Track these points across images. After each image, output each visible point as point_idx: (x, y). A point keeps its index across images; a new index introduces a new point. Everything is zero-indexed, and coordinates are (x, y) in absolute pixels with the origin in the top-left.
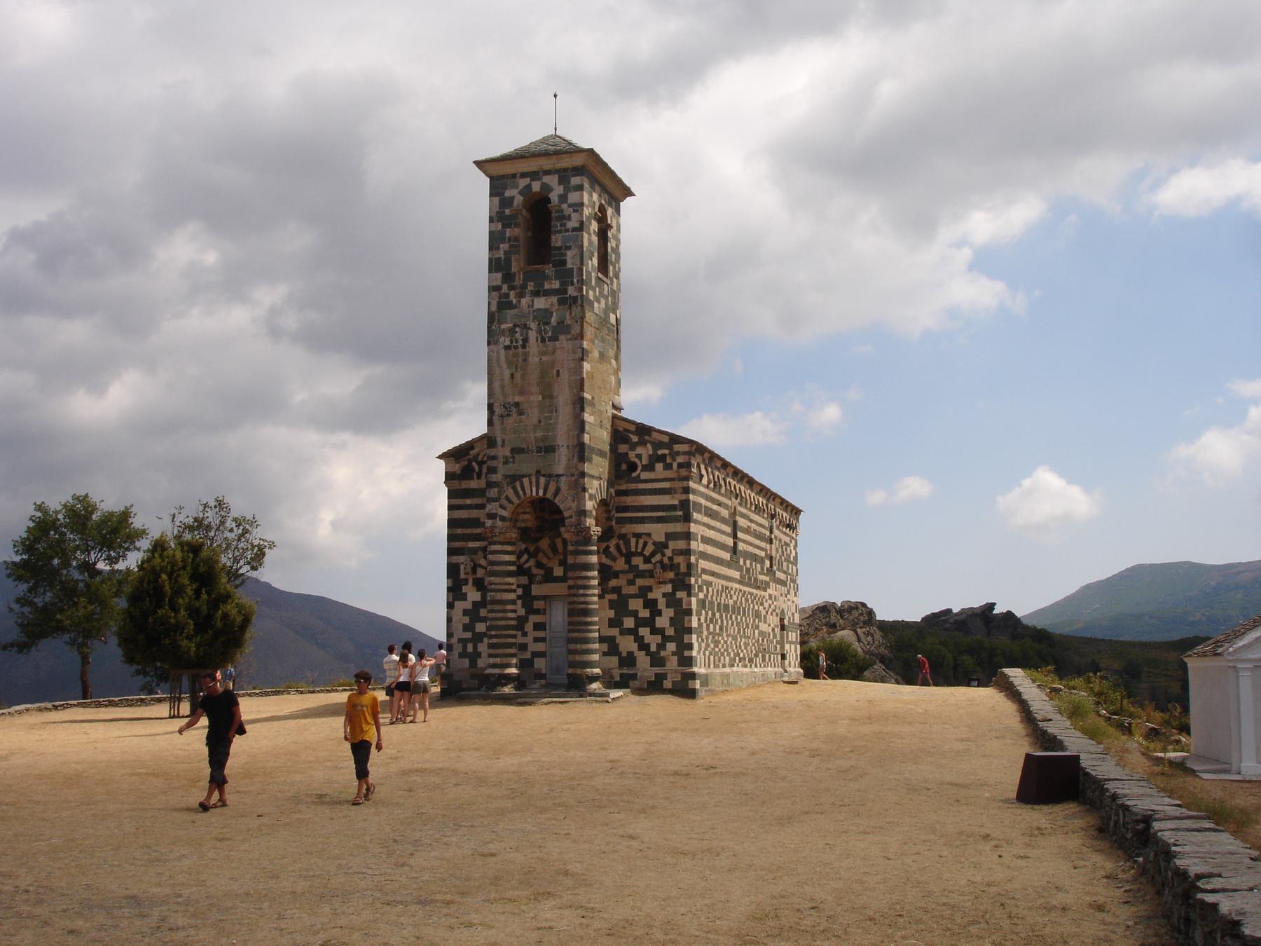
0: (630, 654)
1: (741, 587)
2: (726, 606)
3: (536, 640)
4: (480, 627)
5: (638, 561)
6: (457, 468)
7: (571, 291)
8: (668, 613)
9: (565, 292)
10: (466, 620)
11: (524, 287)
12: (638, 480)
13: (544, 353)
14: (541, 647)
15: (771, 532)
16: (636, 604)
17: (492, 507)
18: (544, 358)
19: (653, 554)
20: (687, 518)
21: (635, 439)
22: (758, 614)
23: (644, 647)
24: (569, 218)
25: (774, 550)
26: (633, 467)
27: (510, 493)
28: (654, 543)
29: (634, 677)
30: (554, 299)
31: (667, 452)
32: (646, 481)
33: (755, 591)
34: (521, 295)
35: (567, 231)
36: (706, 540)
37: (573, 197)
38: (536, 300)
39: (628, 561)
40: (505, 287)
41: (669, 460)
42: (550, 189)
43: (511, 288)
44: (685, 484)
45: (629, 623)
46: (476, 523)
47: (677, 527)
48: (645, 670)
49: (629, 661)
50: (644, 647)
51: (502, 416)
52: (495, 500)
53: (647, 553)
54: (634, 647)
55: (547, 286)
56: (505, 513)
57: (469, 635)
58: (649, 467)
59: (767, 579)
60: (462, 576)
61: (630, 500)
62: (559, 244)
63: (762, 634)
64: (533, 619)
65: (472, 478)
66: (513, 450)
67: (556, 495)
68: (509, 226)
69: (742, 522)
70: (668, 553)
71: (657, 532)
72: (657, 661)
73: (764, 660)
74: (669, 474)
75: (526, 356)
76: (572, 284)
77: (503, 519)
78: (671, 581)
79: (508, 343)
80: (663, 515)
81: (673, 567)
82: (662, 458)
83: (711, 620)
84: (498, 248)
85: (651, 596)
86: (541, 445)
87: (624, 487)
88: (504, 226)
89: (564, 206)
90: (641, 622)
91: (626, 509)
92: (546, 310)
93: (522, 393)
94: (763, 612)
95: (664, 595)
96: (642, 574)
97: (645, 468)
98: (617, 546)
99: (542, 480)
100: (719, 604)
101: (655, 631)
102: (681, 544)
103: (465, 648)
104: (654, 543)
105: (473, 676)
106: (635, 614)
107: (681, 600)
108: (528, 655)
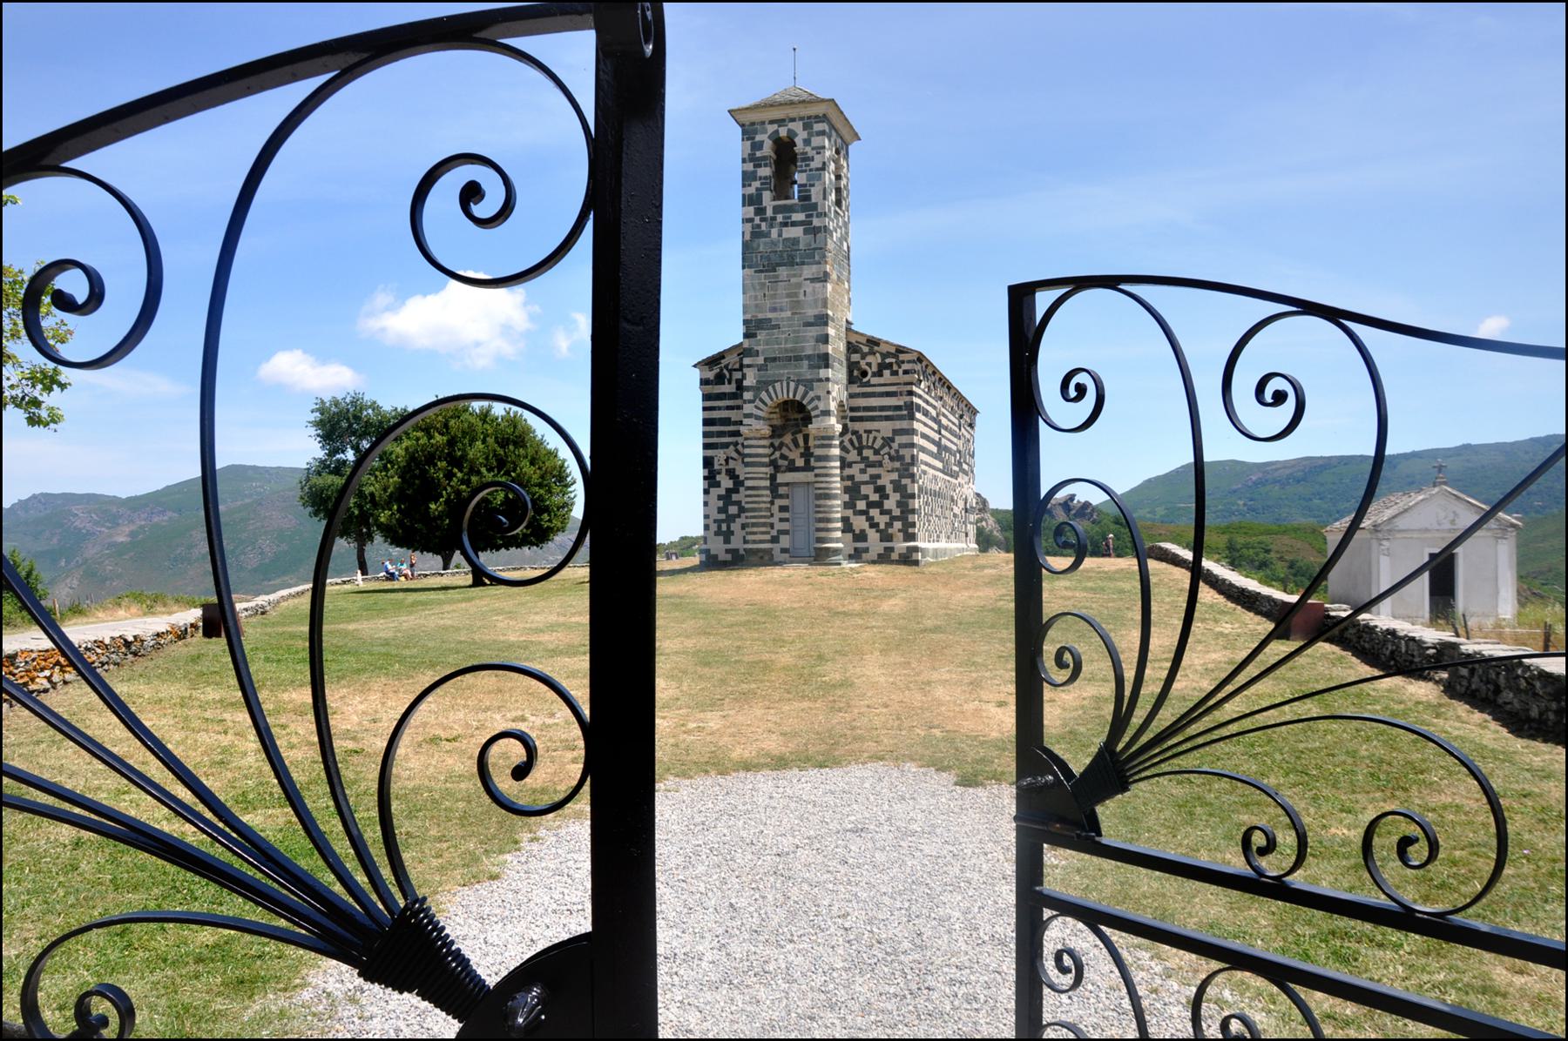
0: (863, 531)
3: (781, 520)
4: (733, 510)
5: (867, 453)
6: (711, 375)
7: (816, 222)
10: (721, 503)
11: (774, 219)
12: (868, 384)
14: (785, 526)
16: (867, 490)
17: (748, 408)
19: (883, 446)
20: (912, 417)
21: (866, 349)
23: (874, 525)
24: (812, 159)
25: (960, 443)
26: (864, 374)
27: (764, 395)
29: (866, 550)
34: (771, 226)
36: (924, 436)
37: (816, 141)
39: (860, 454)
41: (895, 367)
42: (796, 135)
43: (762, 220)
44: (908, 388)
45: (861, 505)
46: (726, 421)
47: (904, 424)
49: (861, 537)
50: (874, 525)
52: (750, 402)
53: (877, 446)
54: (866, 526)
56: (759, 413)
58: (879, 374)
60: (716, 467)
64: (779, 502)
69: (944, 421)
70: (895, 446)
71: (886, 428)
72: (886, 537)
74: (894, 379)
81: (900, 458)
85: (880, 482)
89: (808, 149)
90: (871, 505)
96: (872, 465)
97: (874, 375)
98: (851, 441)
99: (792, 385)
103: (719, 527)
106: (866, 497)
108: (774, 533)
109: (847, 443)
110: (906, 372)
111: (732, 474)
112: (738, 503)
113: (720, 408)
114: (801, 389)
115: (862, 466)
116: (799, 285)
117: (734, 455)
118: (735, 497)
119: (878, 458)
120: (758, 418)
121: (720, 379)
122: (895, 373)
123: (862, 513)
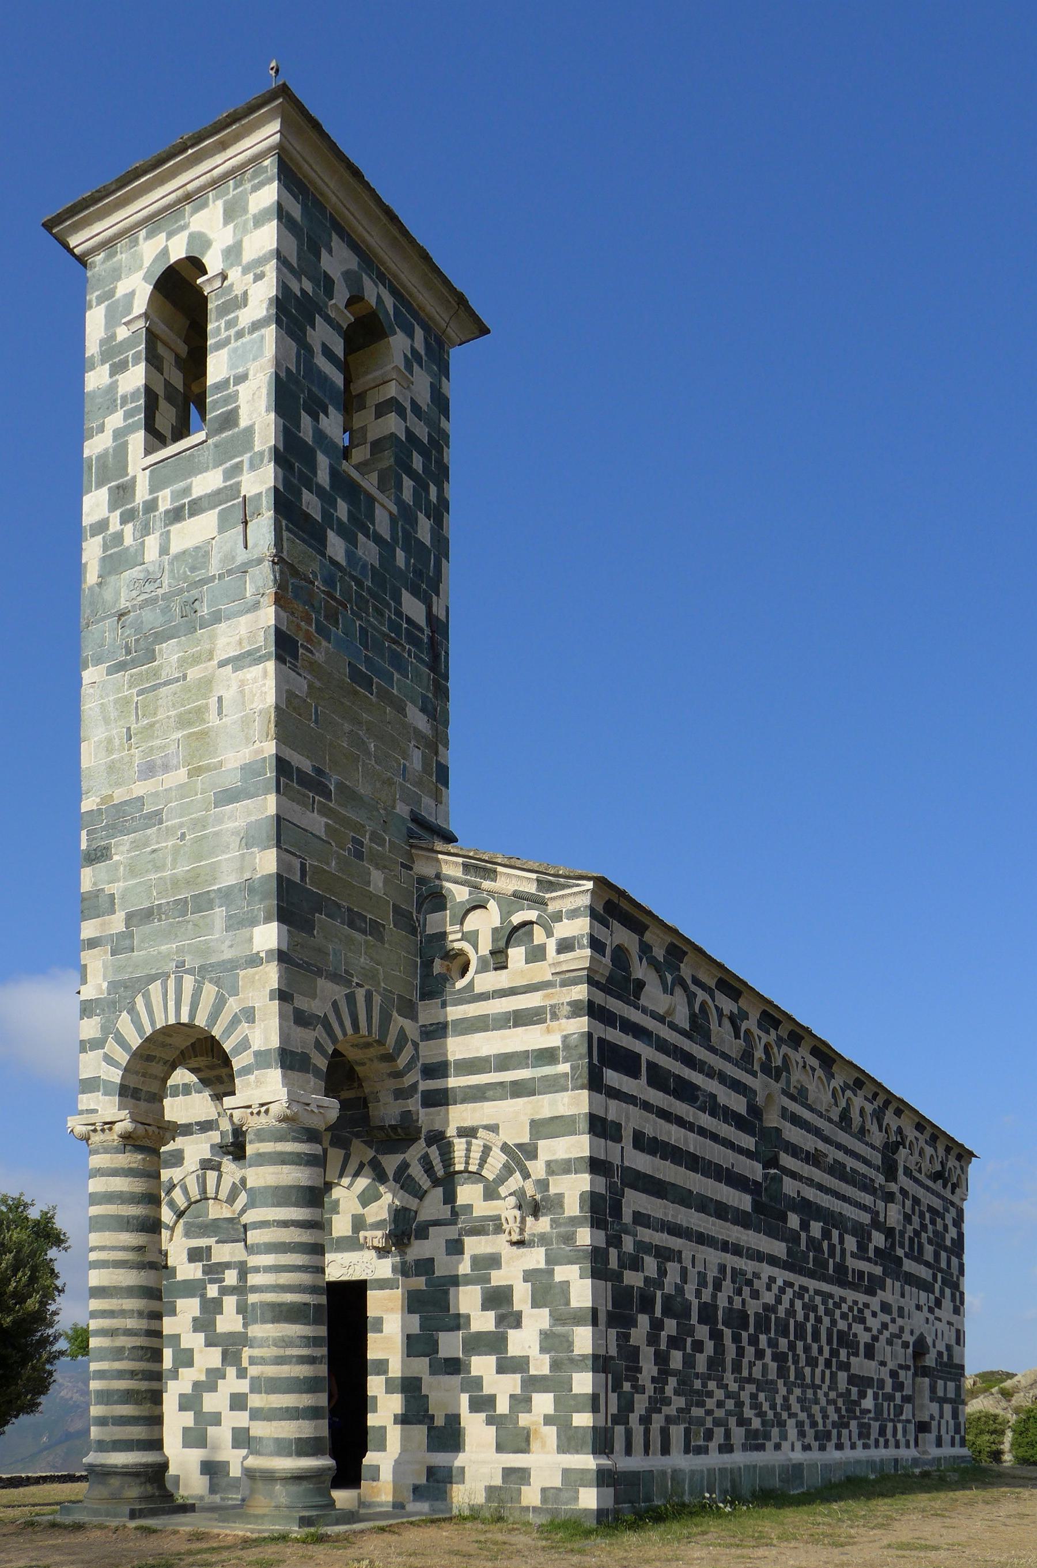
1: (791, 1276)
2: (738, 1319)
8: (537, 1320)
15: (890, 1170)
22: (846, 1340)
23: (483, 1403)
33: (837, 1291)
59: (878, 1270)
63: (862, 1382)
70: (537, 1168)
71: (512, 1119)
73: (864, 1432)
83: (675, 1342)
94: (864, 1338)
95: (529, 1276)
100: (707, 1314)
104: (505, 1148)
109: (416, 1171)
110: (565, 946)
114: (210, 991)
116: (206, 684)
122: (536, 954)
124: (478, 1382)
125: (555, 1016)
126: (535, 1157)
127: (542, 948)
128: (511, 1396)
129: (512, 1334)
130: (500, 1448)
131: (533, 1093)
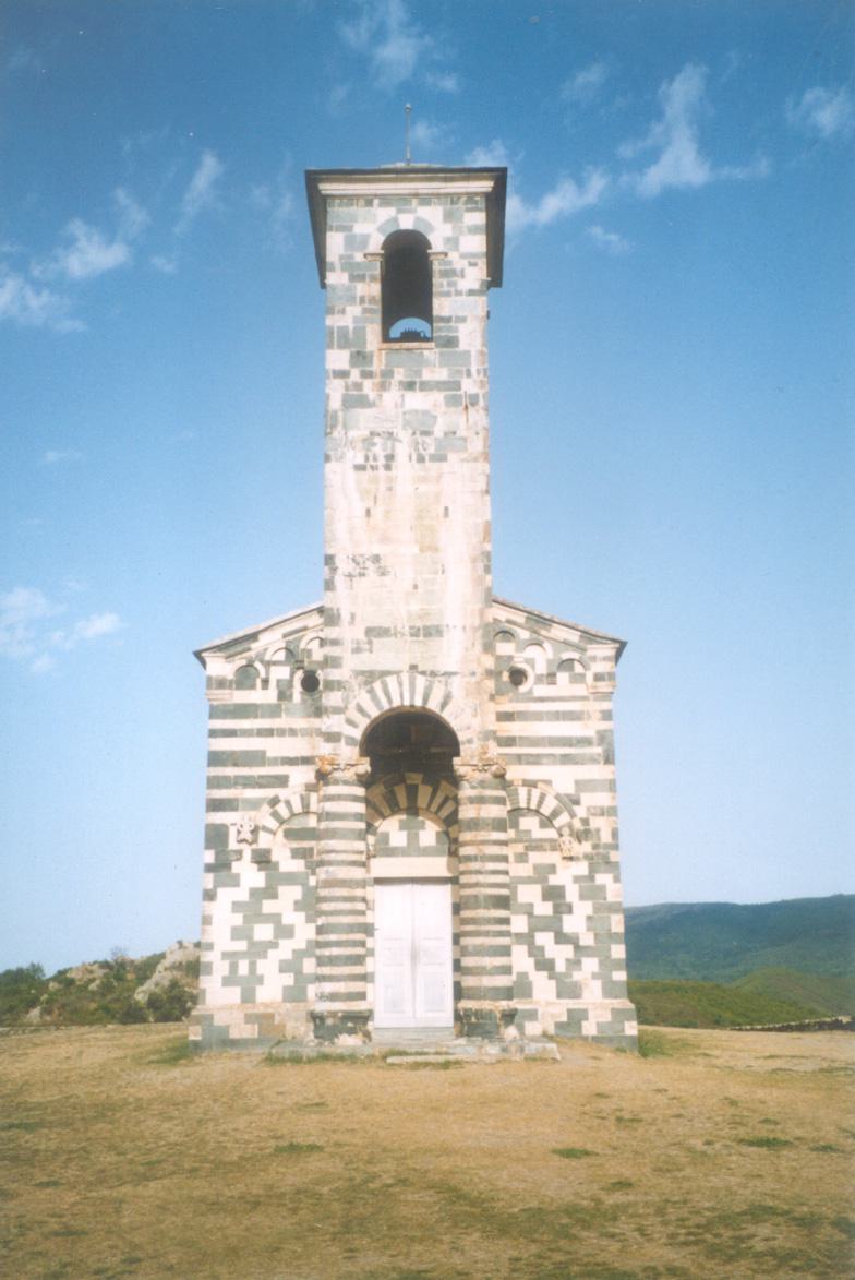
4: (263, 932)
8: (583, 909)
9: (457, 386)
11: (387, 374)
12: (529, 697)
13: (424, 480)
16: (529, 894)
18: (423, 488)
19: (555, 814)
23: (545, 965)
27: (364, 698)
28: (558, 797)
30: (438, 397)
31: (575, 655)
32: (542, 699)
35: (459, 293)
38: (409, 395)
40: (355, 375)
41: (578, 668)
43: (367, 375)
45: (519, 924)
46: (257, 758)
48: (549, 1004)
50: (545, 965)
51: (350, 576)
52: (338, 710)
55: (427, 375)
57: (242, 946)
58: (551, 678)
60: (233, 845)
61: (513, 729)
62: (445, 313)
65: (253, 687)
66: (369, 631)
67: (444, 705)
68: (361, 278)
70: (581, 811)
71: (563, 779)
72: (568, 990)
75: (390, 480)
76: (469, 374)
77: (350, 741)
78: (587, 857)
79: (360, 460)
80: (568, 752)
82: (566, 665)
84: (343, 312)
85: (553, 880)
86: (419, 624)
87: (508, 707)
88: (354, 278)
89: (453, 256)
90: (538, 925)
91: (510, 741)
92: (426, 413)
93: (385, 539)
95: (577, 879)
96: (537, 846)
97: (539, 679)
101: (561, 938)
102: (602, 799)
103: (234, 967)
104: (558, 797)
105: (249, 1019)
106: (528, 910)
107: (602, 888)
111: (263, 860)
112: (275, 919)
113: (247, 733)
115: (520, 848)
117: (272, 823)
118: (268, 906)
119: (551, 833)
120: (350, 741)
121: (245, 678)
122: (580, 679)
123: (519, 937)
124: (542, 949)
125: (589, 717)
126: (577, 802)
127: (583, 676)
128: (568, 960)
129: (565, 918)
130: (559, 996)
131: (576, 763)
